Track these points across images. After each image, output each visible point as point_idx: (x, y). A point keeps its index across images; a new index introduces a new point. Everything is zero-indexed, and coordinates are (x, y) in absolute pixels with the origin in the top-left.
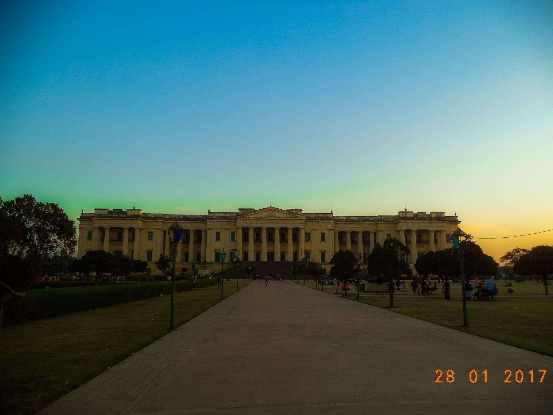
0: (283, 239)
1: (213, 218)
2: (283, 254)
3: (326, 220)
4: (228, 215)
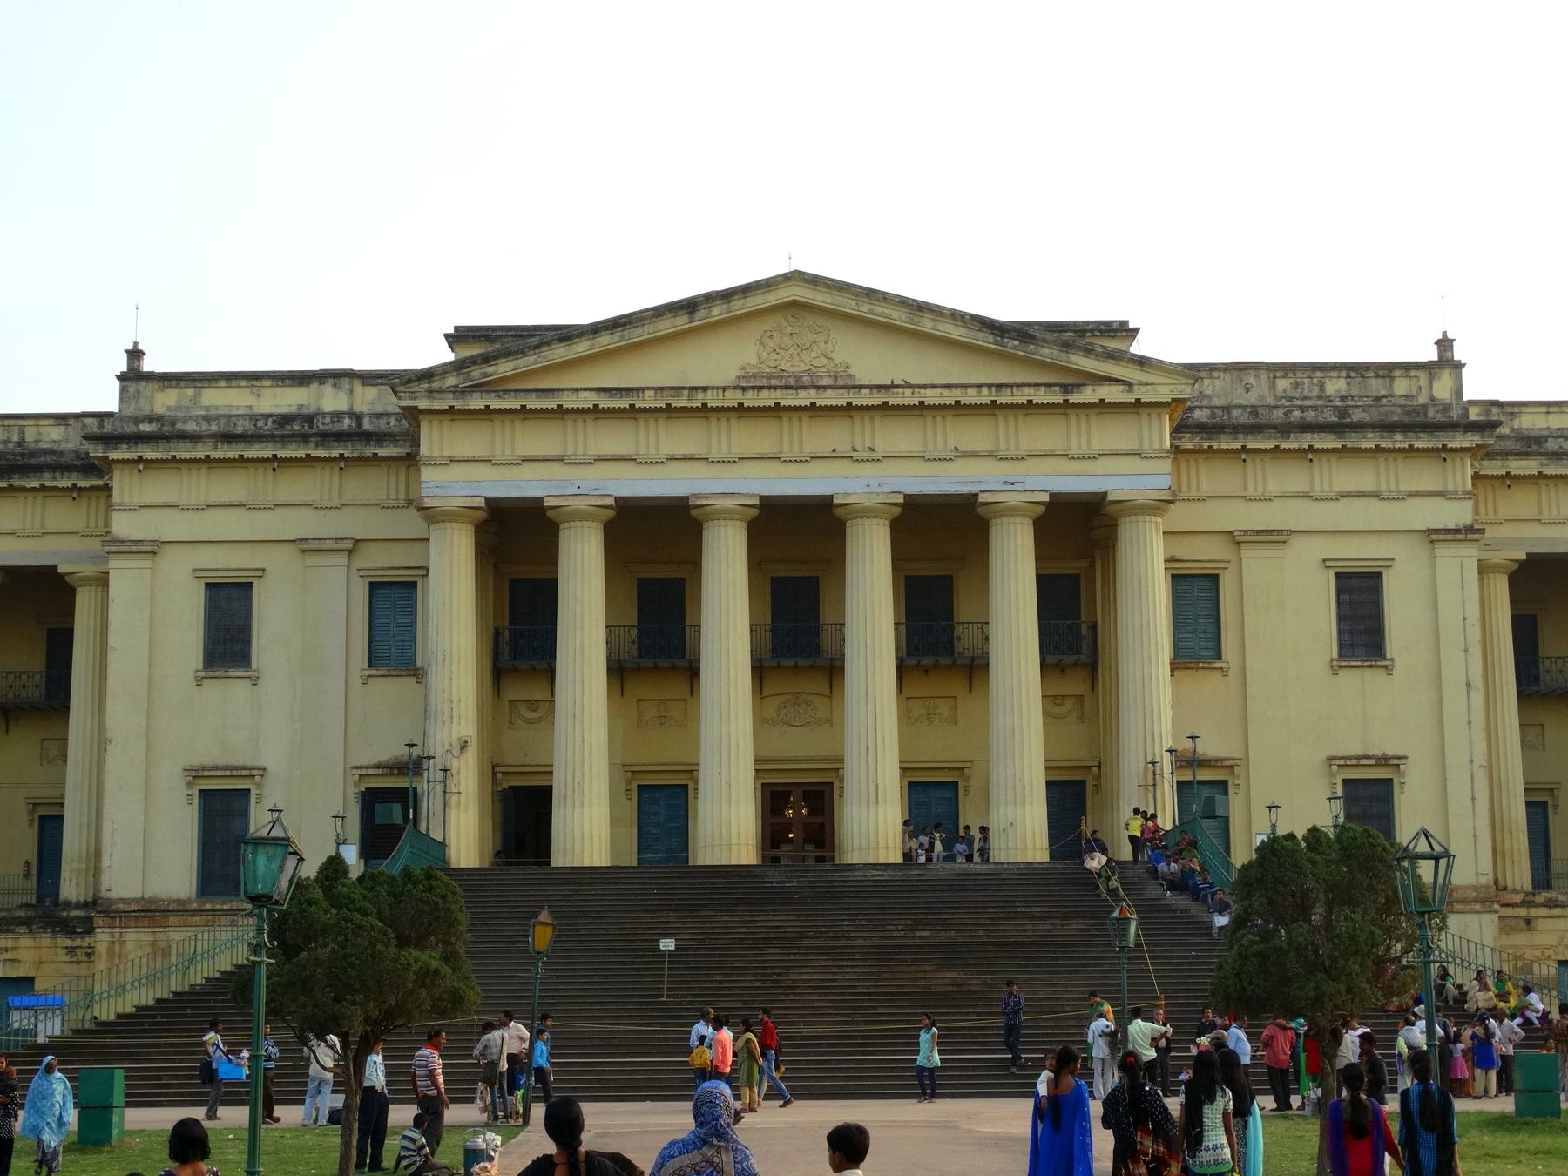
0: (938, 643)
1: (167, 433)
2: (934, 802)
3: (1388, 427)
4: (331, 400)
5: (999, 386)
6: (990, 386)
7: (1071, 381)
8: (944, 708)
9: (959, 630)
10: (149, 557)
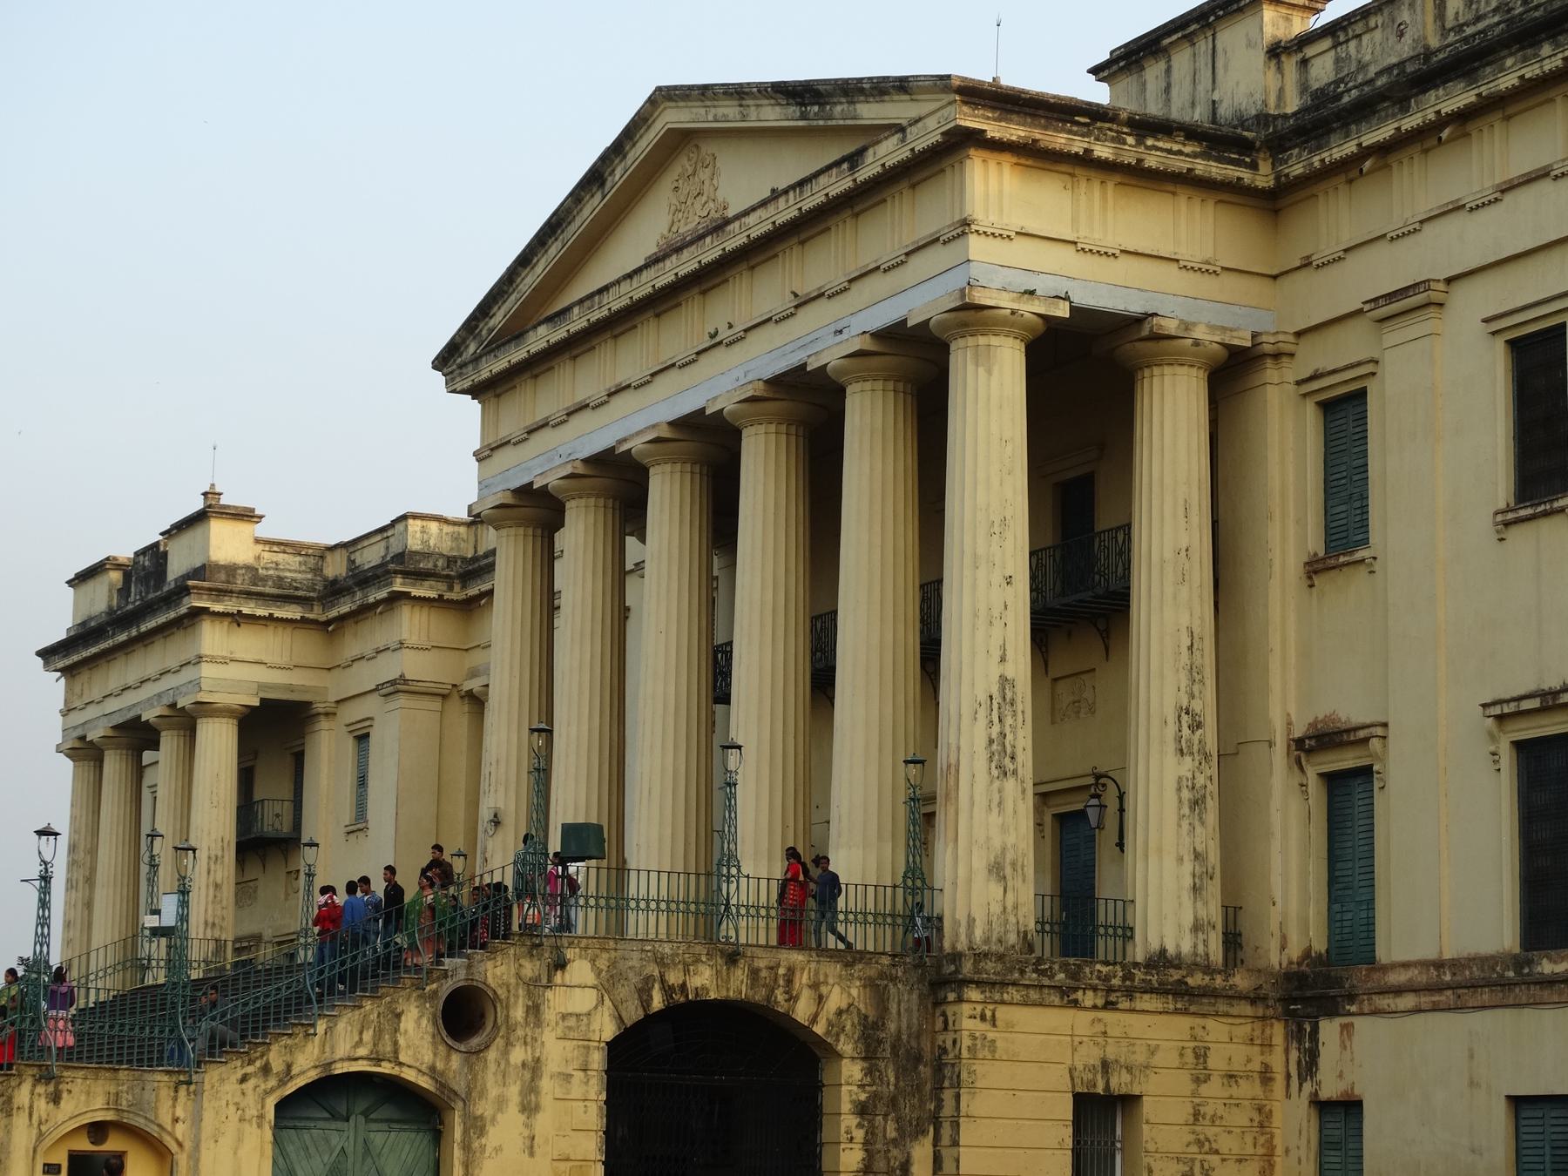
7: (849, 148)
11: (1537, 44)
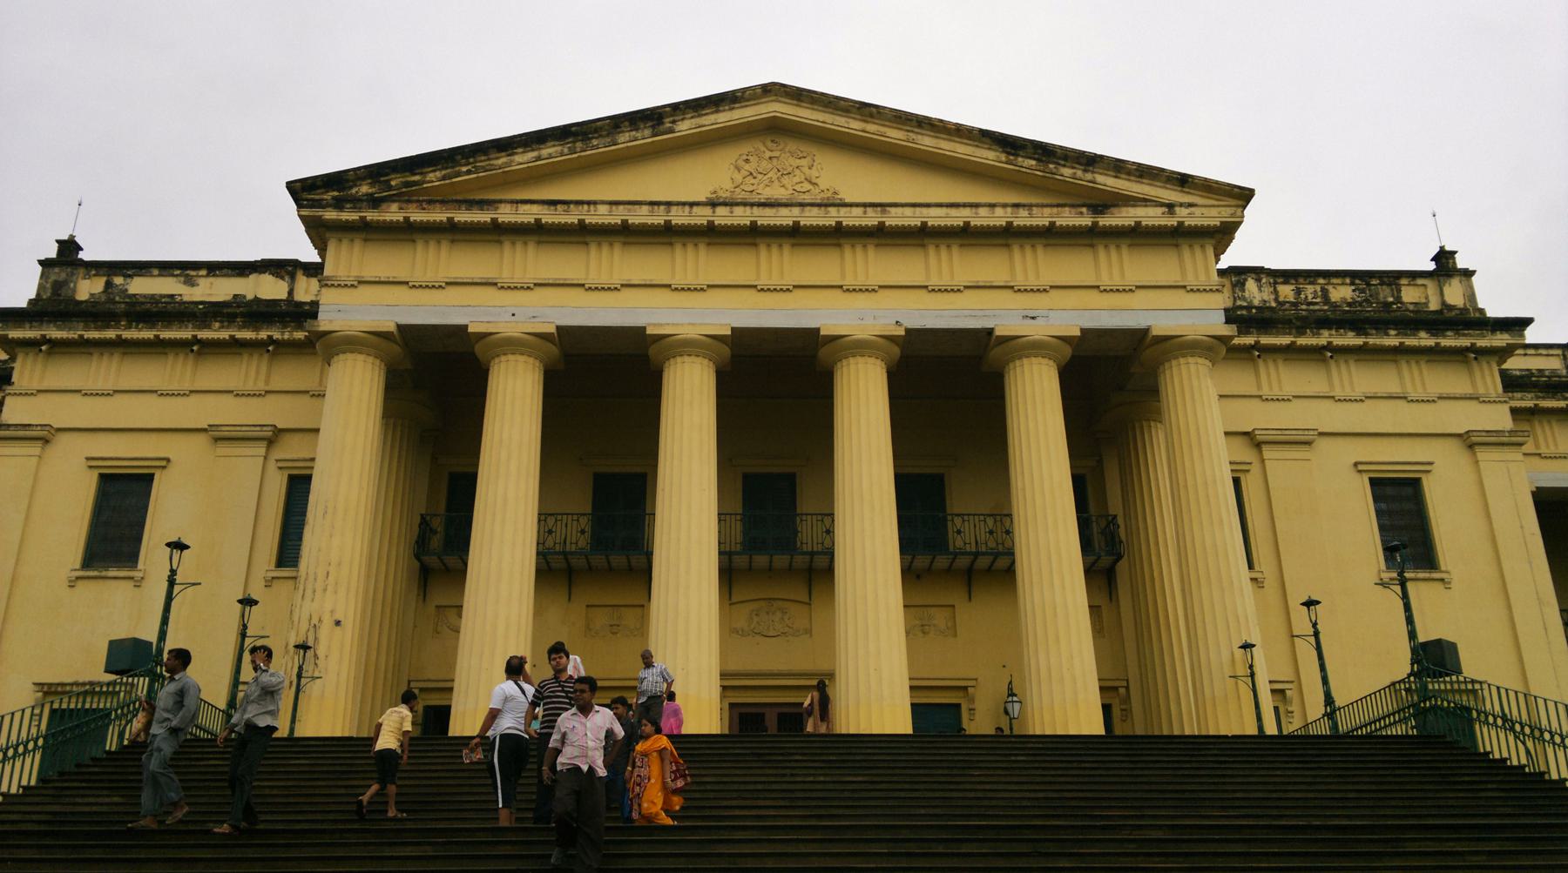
5: (1016, 206)
6: (1005, 206)
8: (940, 618)
9: (958, 521)
10: (39, 444)
11: (1418, 329)
